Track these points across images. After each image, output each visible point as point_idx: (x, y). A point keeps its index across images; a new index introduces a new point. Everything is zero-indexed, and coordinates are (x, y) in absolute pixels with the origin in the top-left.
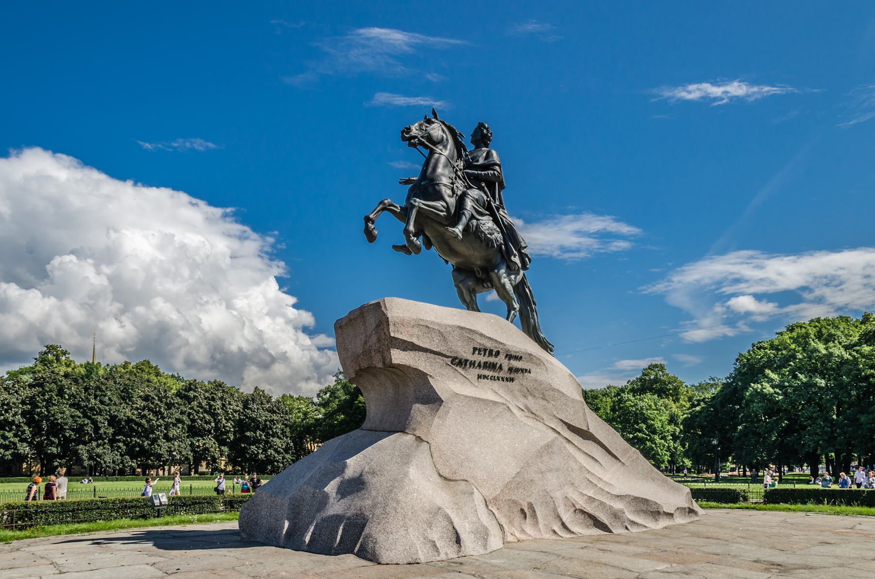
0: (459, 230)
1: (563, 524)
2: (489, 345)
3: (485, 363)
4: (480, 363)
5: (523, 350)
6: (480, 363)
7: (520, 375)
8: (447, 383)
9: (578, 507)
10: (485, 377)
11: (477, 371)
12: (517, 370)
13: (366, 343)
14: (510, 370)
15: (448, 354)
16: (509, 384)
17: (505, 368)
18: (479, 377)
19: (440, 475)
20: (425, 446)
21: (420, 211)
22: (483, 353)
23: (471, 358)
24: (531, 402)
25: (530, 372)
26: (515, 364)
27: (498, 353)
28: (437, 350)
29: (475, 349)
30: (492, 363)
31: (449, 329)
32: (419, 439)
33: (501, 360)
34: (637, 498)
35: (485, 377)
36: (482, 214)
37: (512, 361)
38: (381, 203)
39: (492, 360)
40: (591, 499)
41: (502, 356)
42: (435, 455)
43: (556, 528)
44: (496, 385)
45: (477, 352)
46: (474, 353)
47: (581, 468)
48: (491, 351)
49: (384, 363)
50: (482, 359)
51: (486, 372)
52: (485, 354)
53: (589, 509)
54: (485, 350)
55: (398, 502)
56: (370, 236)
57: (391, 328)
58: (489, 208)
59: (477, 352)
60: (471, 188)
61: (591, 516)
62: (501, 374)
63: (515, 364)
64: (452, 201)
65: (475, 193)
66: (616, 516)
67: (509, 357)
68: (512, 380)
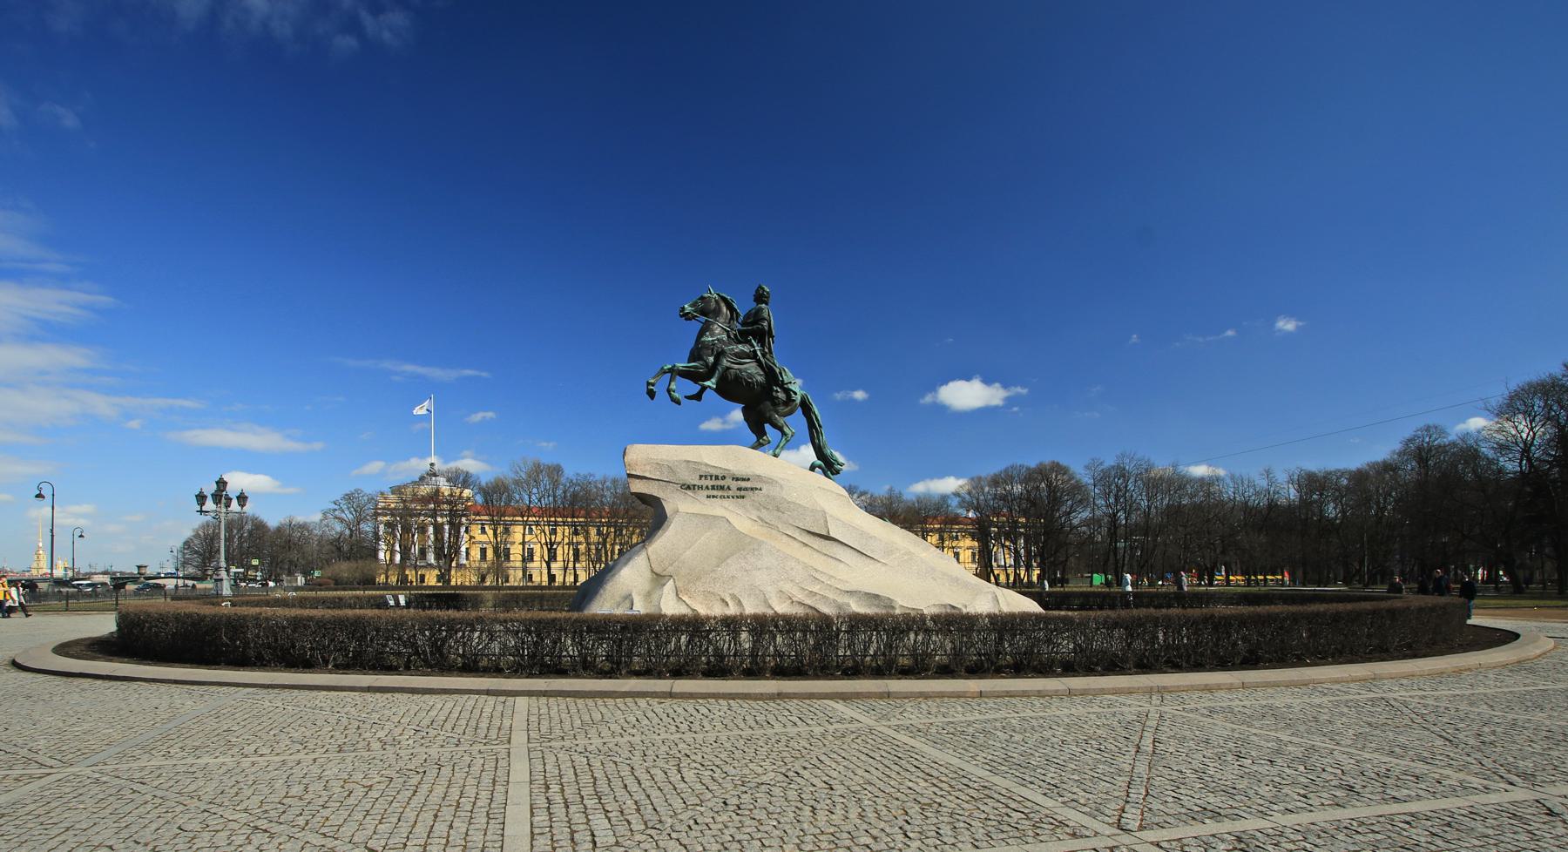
2: (714, 472)
3: (713, 488)
8: (675, 503)
11: (706, 492)
23: (697, 482)
24: (764, 514)
27: (724, 478)
30: (720, 485)
33: (728, 482)
44: (726, 503)
47: (806, 567)
50: (710, 483)
51: (715, 493)
56: (651, 394)
58: (754, 355)
64: (711, 359)
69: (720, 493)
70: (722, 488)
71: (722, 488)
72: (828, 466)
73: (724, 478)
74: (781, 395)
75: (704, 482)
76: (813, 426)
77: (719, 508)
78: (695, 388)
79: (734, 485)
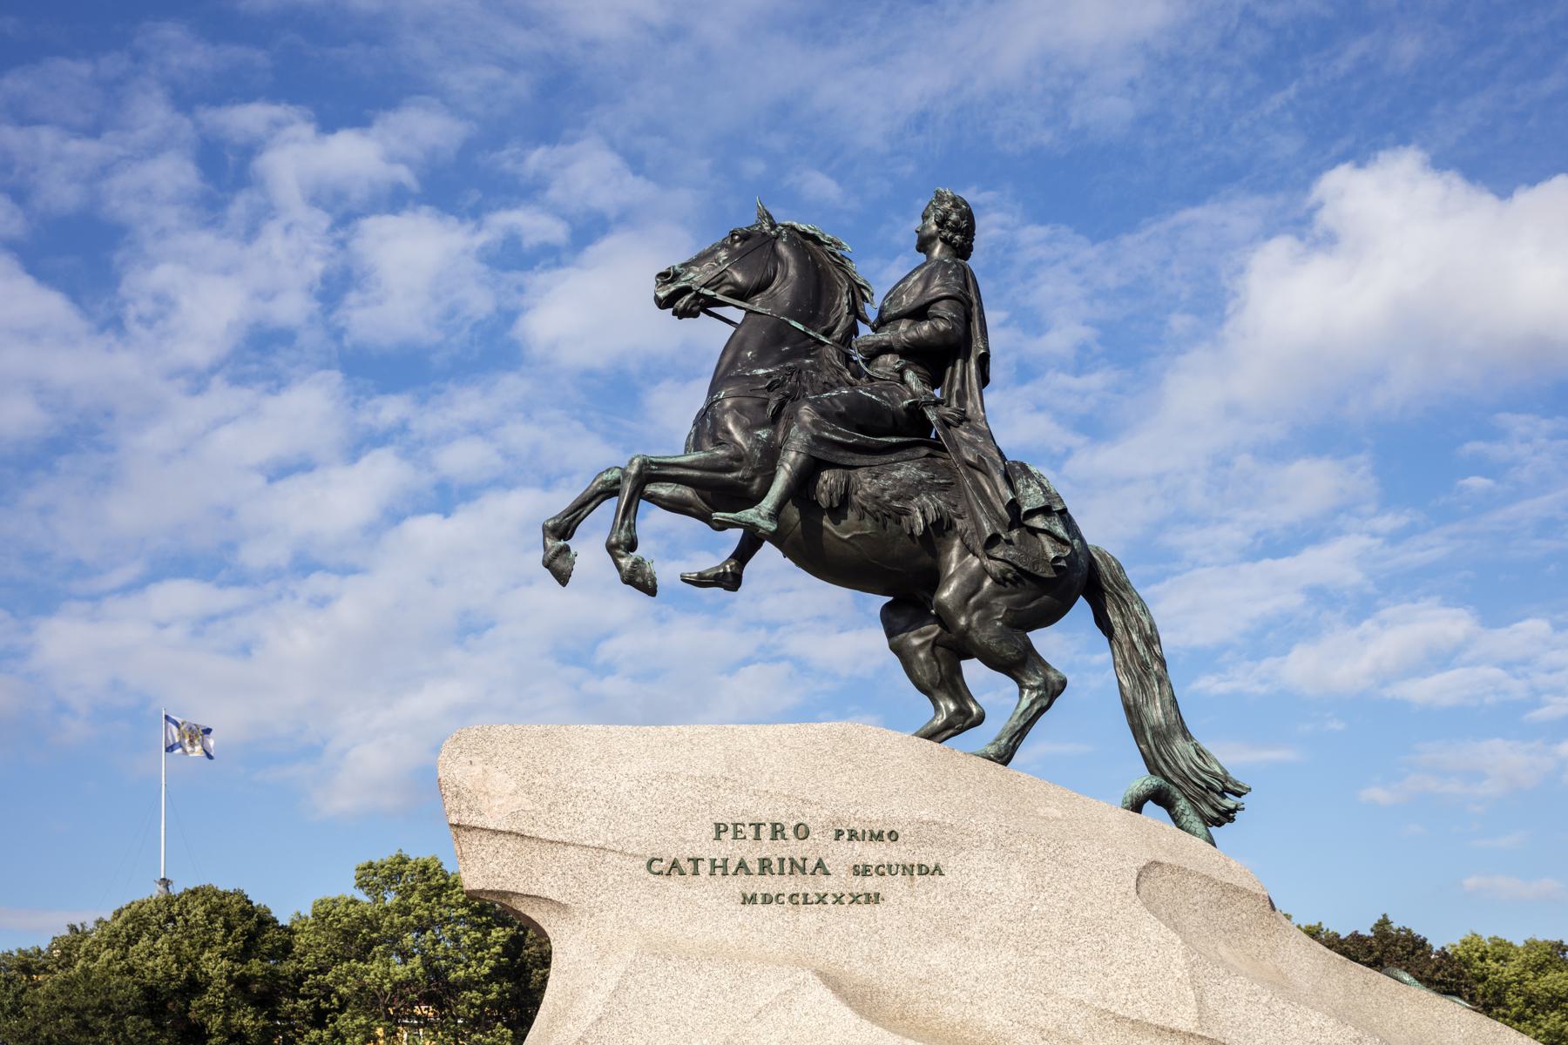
2: (765, 814)
3: (765, 865)
4: (742, 865)
5: (899, 813)
6: (742, 865)
7: (900, 881)
11: (738, 884)
12: (884, 870)
14: (862, 871)
15: (636, 850)
16: (864, 910)
22: (751, 832)
25: (938, 870)
26: (872, 853)
27: (802, 832)
28: (597, 843)
29: (719, 829)
31: (626, 785)
35: (767, 900)
37: (857, 845)
39: (792, 848)
44: (809, 917)
45: (729, 835)
46: (718, 838)
48: (777, 831)
50: (752, 852)
51: (769, 884)
52: (757, 838)
54: (758, 826)
57: (451, 803)
59: (729, 835)
62: (828, 885)
63: (872, 853)
67: (853, 835)
68: (873, 898)
69: (788, 884)
70: (798, 867)
71: (798, 867)
72: (1190, 793)
73: (802, 832)
75: (727, 849)
76: (1144, 663)
78: (717, 549)
79: (842, 855)
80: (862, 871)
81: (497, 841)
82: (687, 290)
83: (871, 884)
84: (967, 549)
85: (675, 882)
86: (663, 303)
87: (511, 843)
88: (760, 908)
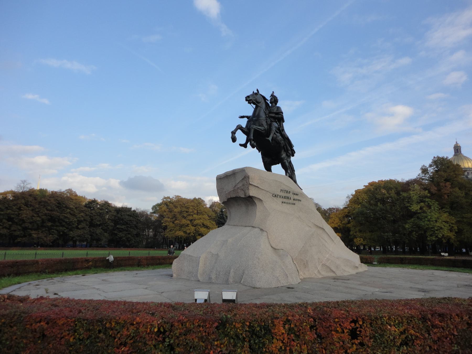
0: (270, 139)
1: (318, 271)
2: (286, 189)
9: (323, 262)
10: (285, 203)
13: (235, 186)
14: (294, 200)
17: (292, 199)
18: (282, 202)
19: (272, 247)
20: (265, 234)
21: (256, 131)
26: (296, 197)
32: (262, 230)
33: (291, 195)
34: (345, 259)
35: (285, 203)
36: (277, 132)
38: (237, 126)
40: (328, 260)
41: (291, 194)
42: (269, 237)
43: (316, 273)
44: (289, 206)
48: (287, 192)
49: (245, 195)
53: (327, 264)
55: (259, 259)
60: (272, 121)
61: (328, 267)
63: (296, 197)
65: (275, 125)
66: (337, 267)
68: (294, 204)
70: (288, 198)
74: (290, 152)
77: (286, 208)
80: (294, 200)
81: (255, 188)
82: (251, 100)
83: (295, 202)
84: (285, 151)
85: (275, 198)
86: (246, 100)
87: (257, 188)
88: (283, 204)
